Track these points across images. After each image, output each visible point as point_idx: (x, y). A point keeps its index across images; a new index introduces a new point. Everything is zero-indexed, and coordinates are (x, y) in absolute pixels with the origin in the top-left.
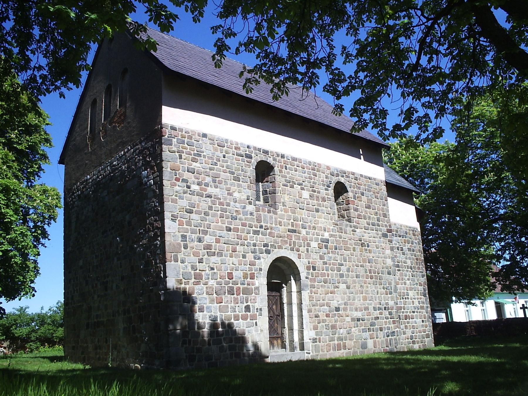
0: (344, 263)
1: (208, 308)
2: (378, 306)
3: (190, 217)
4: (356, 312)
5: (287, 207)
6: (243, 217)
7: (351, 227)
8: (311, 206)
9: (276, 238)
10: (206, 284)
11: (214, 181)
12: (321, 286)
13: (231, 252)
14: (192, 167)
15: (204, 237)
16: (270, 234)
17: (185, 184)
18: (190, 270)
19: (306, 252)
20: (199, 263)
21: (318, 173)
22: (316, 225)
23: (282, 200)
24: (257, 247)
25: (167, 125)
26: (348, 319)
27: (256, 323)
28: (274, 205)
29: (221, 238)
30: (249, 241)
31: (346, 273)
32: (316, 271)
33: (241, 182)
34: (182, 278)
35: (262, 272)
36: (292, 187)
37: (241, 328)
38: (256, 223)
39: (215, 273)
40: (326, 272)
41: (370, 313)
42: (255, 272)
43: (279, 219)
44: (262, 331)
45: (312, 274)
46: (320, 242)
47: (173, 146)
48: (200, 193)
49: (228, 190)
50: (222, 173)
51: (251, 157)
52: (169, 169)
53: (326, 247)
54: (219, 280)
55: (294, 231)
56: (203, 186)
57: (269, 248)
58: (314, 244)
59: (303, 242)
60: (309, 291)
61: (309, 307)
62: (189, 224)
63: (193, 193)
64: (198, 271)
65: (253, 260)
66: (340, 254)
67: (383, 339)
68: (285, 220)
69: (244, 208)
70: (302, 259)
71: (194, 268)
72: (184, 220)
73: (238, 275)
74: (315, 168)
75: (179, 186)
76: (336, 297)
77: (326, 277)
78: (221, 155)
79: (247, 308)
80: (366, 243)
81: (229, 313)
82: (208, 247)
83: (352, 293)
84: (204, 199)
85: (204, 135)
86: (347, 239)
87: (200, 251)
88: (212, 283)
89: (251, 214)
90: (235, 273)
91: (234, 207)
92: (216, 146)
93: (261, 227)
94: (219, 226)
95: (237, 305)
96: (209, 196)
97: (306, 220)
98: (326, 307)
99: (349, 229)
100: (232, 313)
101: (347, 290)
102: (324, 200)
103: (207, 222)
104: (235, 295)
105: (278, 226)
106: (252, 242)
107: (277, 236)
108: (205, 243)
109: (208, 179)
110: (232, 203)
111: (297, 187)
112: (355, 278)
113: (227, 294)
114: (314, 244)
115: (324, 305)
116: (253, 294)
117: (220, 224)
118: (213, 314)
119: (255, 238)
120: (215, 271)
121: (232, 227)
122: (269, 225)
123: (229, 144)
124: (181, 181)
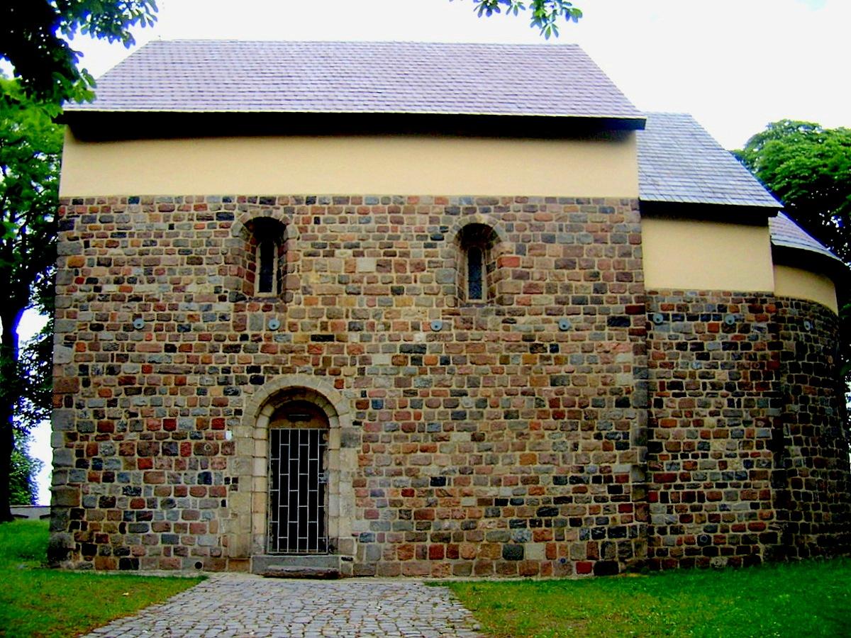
0: (470, 391)
1: (120, 476)
2: (570, 474)
3: (96, 336)
4: (495, 488)
5: (314, 295)
6: (205, 326)
7: (498, 313)
8: (380, 284)
9: (279, 354)
12: (396, 438)
13: (173, 386)
14: (106, 256)
15: (120, 366)
16: (264, 349)
17: (92, 286)
18: (92, 419)
19: (356, 376)
20: (109, 406)
21: (405, 217)
22: (391, 322)
23: (302, 283)
24: (232, 374)
25: (67, 200)
26: (472, 501)
27: (224, 503)
29: (153, 365)
30: (213, 365)
31: (474, 409)
32: (384, 410)
33: (204, 266)
34: (76, 431)
35: (241, 417)
36: (331, 254)
37: (191, 508)
38: (232, 332)
39: (137, 421)
40: (412, 411)
41: (540, 489)
42: (226, 418)
43: (292, 320)
44: (235, 515)
45: (372, 418)
46: (398, 353)
47: (75, 230)
48: (119, 296)
50: (164, 256)
51: (231, 217)
52: (66, 268)
53: (416, 361)
54: (145, 432)
55: (330, 338)
56: (126, 284)
57: (261, 374)
58: (381, 359)
59: (349, 357)
60: (360, 448)
61: (356, 477)
62: (94, 347)
63: (105, 298)
64: (106, 419)
65: (222, 396)
66: (457, 371)
67: (578, 542)
68: (307, 320)
69: (209, 308)
70: (345, 389)
71: (97, 414)
72: (87, 343)
73: (187, 423)
74: (398, 208)
75: (81, 290)
76: (437, 458)
77: (412, 420)
78: (166, 226)
79: (206, 478)
80: (547, 345)
81: (166, 485)
82: (128, 380)
83: (490, 450)
84: (126, 305)
85: (134, 200)
86: (483, 341)
87: (113, 389)
88: (132, 437)
89: (223, 317)
90: (180, 421)
91: (183, 310)
92: (157, 212)
93: (244, 338)
94: (152, 346)
95: (183, 472)
96: (138, 299)
97: (363, 314)
98: (404, 478)
99: (492, 320)
100: (173, 486)
101: (475, 445)
102: (419, 267)
103: (129, 341)
104: (179, 457)
105: (287, 332)
106: (221, 367)
107: (283, 351)
108: (122, 374)
109: (137, 272)
110: (182, 304)
111: (344, 254)
112: (502, 419)
113: (160, 454)
114: (381, 359)
115: (399, 474)
116: (219, 455)
117: (154, 342)
118: (131, 484)
119: (227, 359)
120: (139, 418)
121: (177, 344)
122: (263, 333)
123: (184, 203)
124: (85, 281)
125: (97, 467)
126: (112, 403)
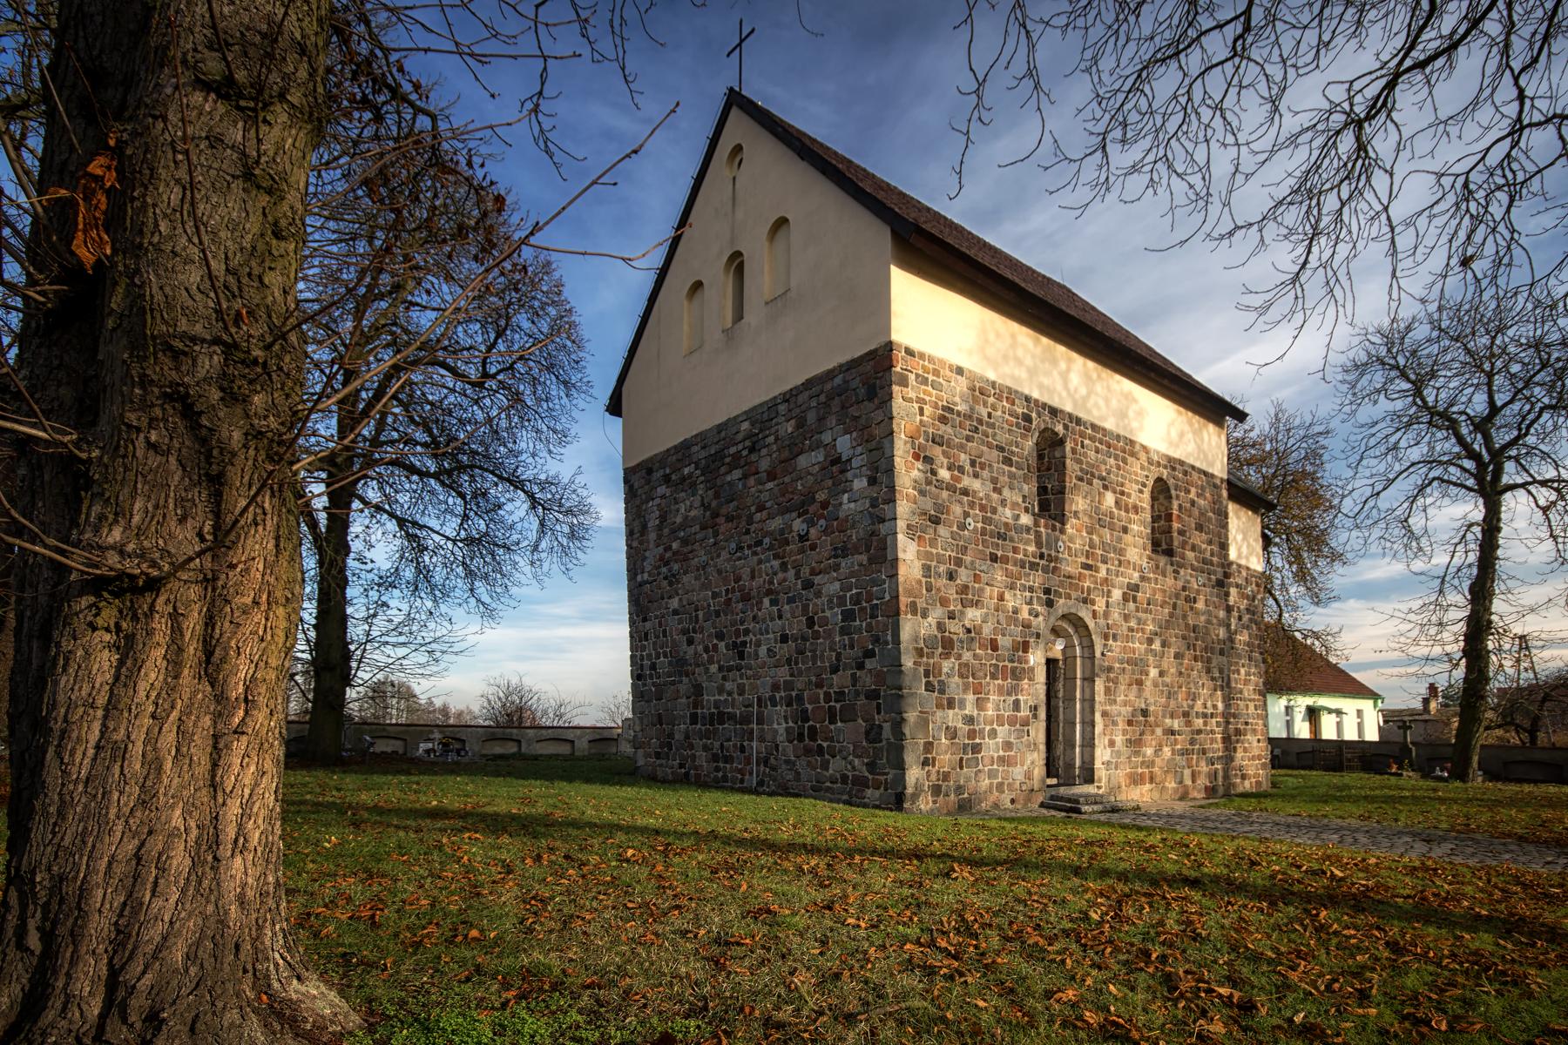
10: (959, 657)
11: (973, 463)
28: (1061, 518)
49: (994, 481)
121: (999, 553)
125: (942, 692)
126: (951, 616)
